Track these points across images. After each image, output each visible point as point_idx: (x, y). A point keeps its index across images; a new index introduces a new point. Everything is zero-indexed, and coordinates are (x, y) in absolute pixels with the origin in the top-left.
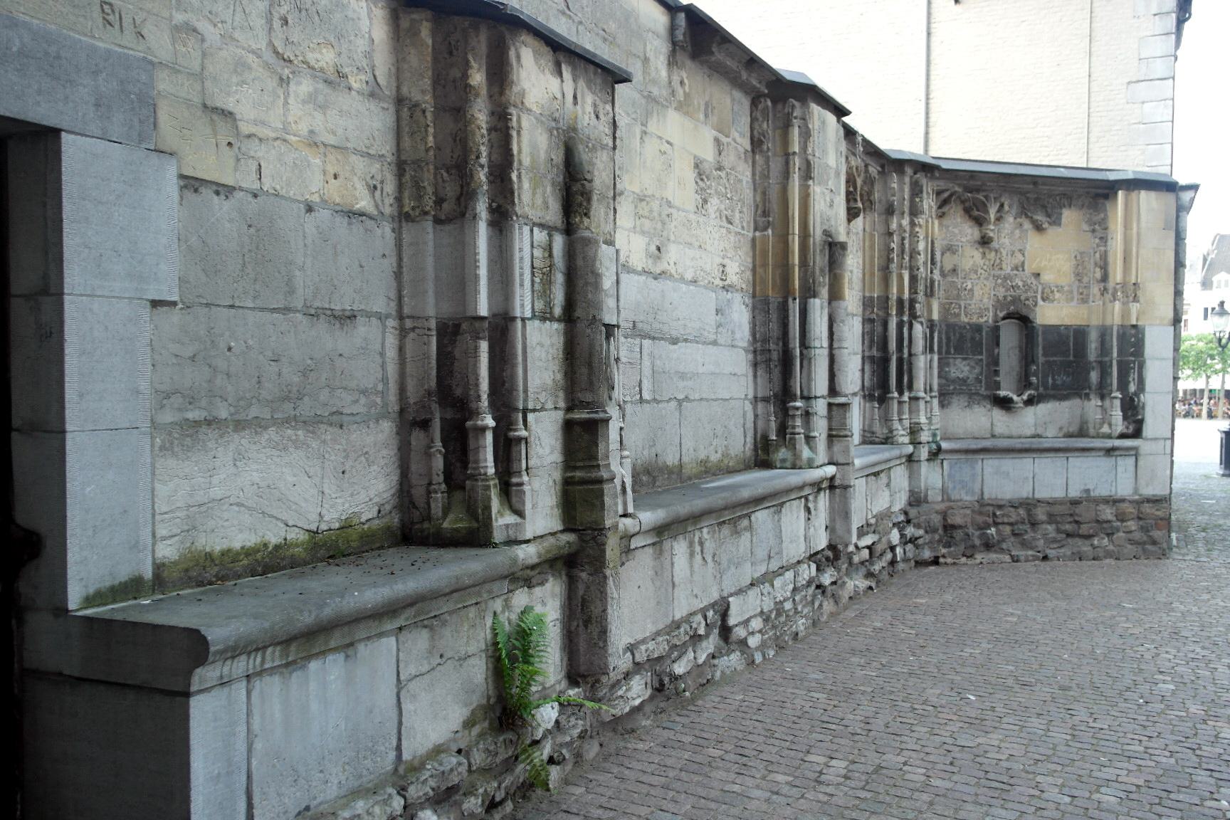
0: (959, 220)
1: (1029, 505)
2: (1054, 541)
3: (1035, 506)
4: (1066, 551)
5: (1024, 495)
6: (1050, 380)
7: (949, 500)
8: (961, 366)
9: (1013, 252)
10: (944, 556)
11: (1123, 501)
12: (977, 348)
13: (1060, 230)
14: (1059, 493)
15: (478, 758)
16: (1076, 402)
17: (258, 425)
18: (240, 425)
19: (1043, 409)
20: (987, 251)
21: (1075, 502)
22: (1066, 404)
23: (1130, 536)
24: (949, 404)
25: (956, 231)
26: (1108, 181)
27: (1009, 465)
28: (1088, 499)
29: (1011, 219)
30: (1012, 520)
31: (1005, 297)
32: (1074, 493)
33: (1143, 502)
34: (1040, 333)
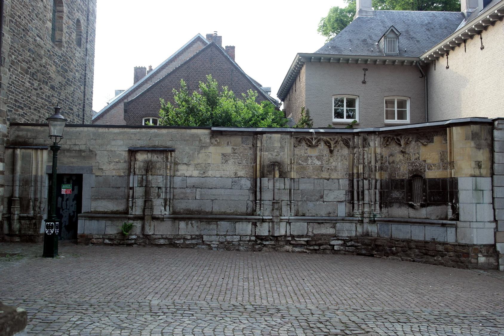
0: (394, 145)
1: (409, 241)
2: (418, 255)
3: (410, 242)
4: (424, 260)
5: (407, 238)
6: (432, 199)
7: (380, 236)
8: (397, 193)
9: (415, 154)
10: (375, 254)
11: (447, 244)
12: (402, 187)
13: (434, 144)
14: (422, 239)
15: (117, 237)
16: (444, 206)
17: (104, 199)
18: (102, 199)
19: (430, 209)
20: (405, 155)
21: (426, 242)
22: (439, 207)
23: (451, 258)
24: (393, 206)
25: (393, 149)
26: (444, 125)
27: (401, 227)
28: (434, 242)
29: (413, 143)
30: (401, 246)
31: (412, 170)
32: (428, 239)
33: (457, 245)
34: (427, 181)
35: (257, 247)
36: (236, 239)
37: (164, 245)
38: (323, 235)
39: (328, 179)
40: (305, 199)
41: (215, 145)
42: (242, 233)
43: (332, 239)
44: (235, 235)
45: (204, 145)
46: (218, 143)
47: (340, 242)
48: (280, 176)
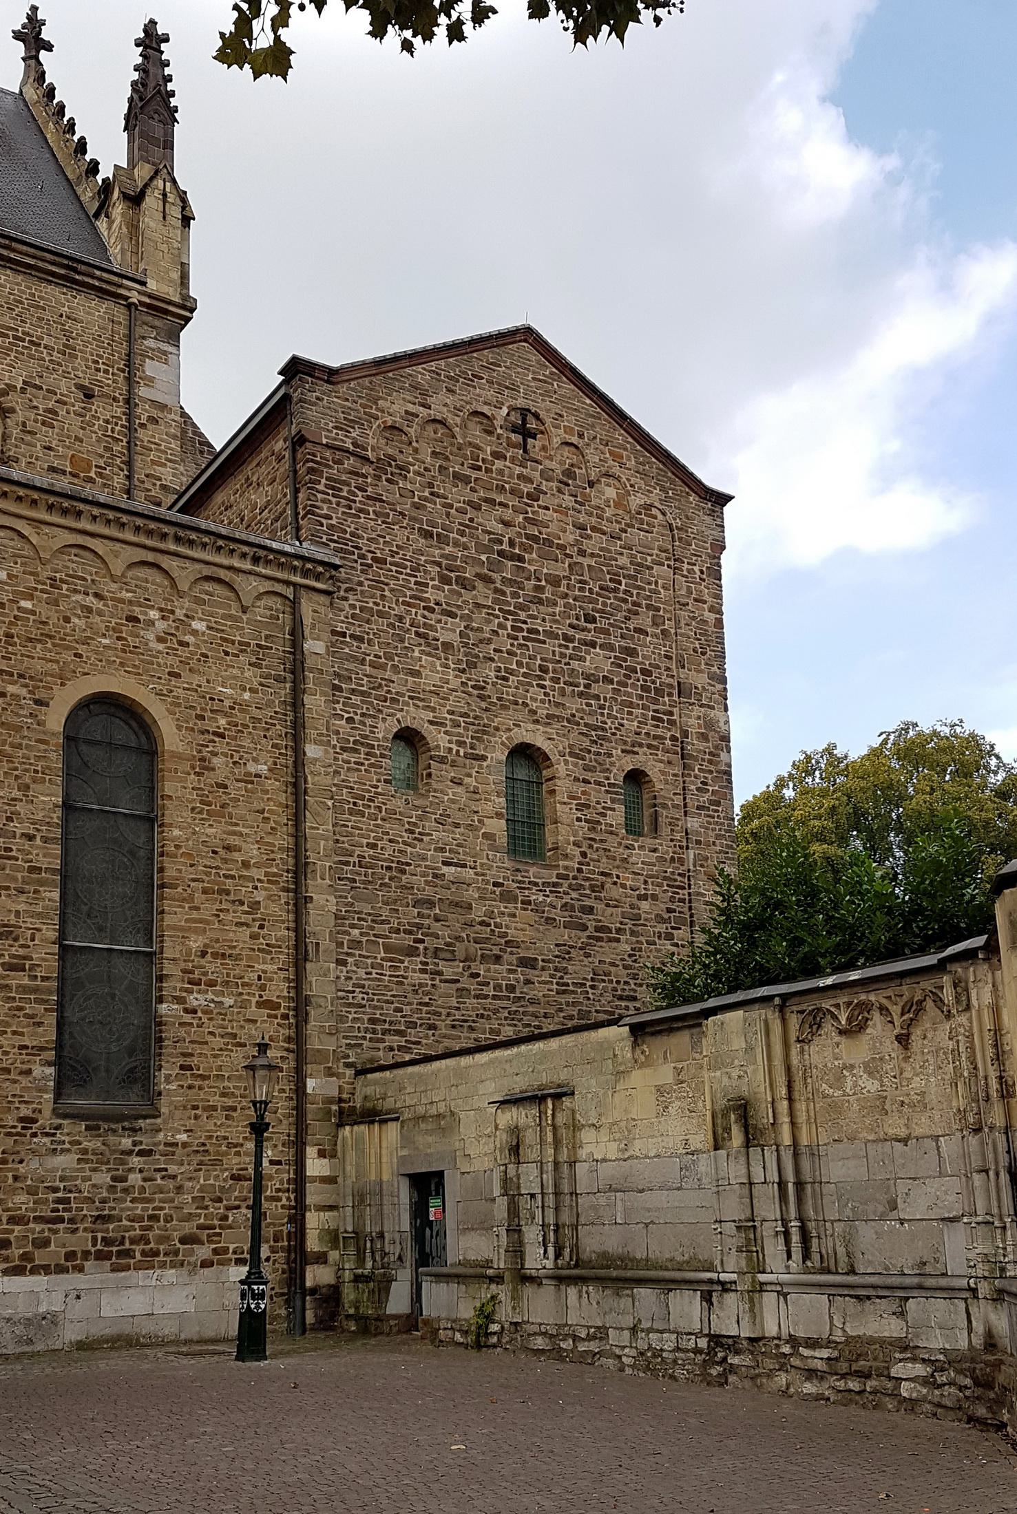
35: (715, 1371)
36: (669, 1342)
37: (542, 1351)
38: (871, 1341)
39: (905, 1141)
40: (848, 1212)
41: (642, 1066)
42: (683, 1325)
43: (897, 1355)
44: (669, 1331)
45: (622, 1069)
46: (646, 1056)
47: (920, 1370)
48: (747, 1144)
